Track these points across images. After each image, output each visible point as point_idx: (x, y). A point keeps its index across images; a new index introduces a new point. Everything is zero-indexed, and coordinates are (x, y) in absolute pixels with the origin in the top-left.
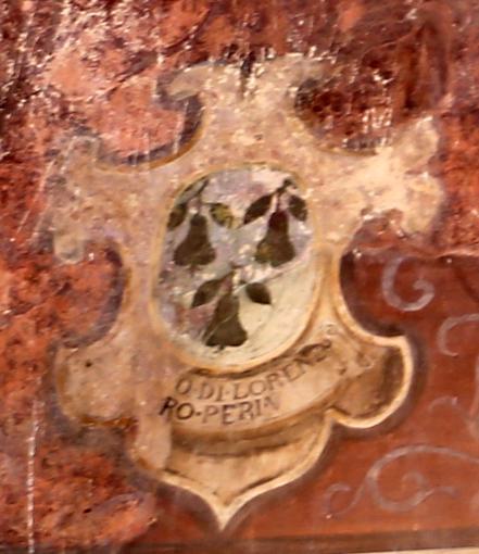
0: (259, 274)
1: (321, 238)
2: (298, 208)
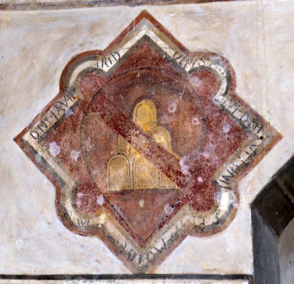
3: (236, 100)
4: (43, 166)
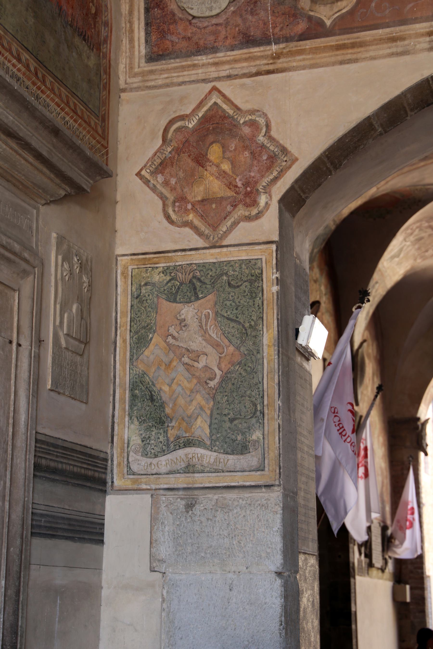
3: (271, 139)
4: (154, 189)
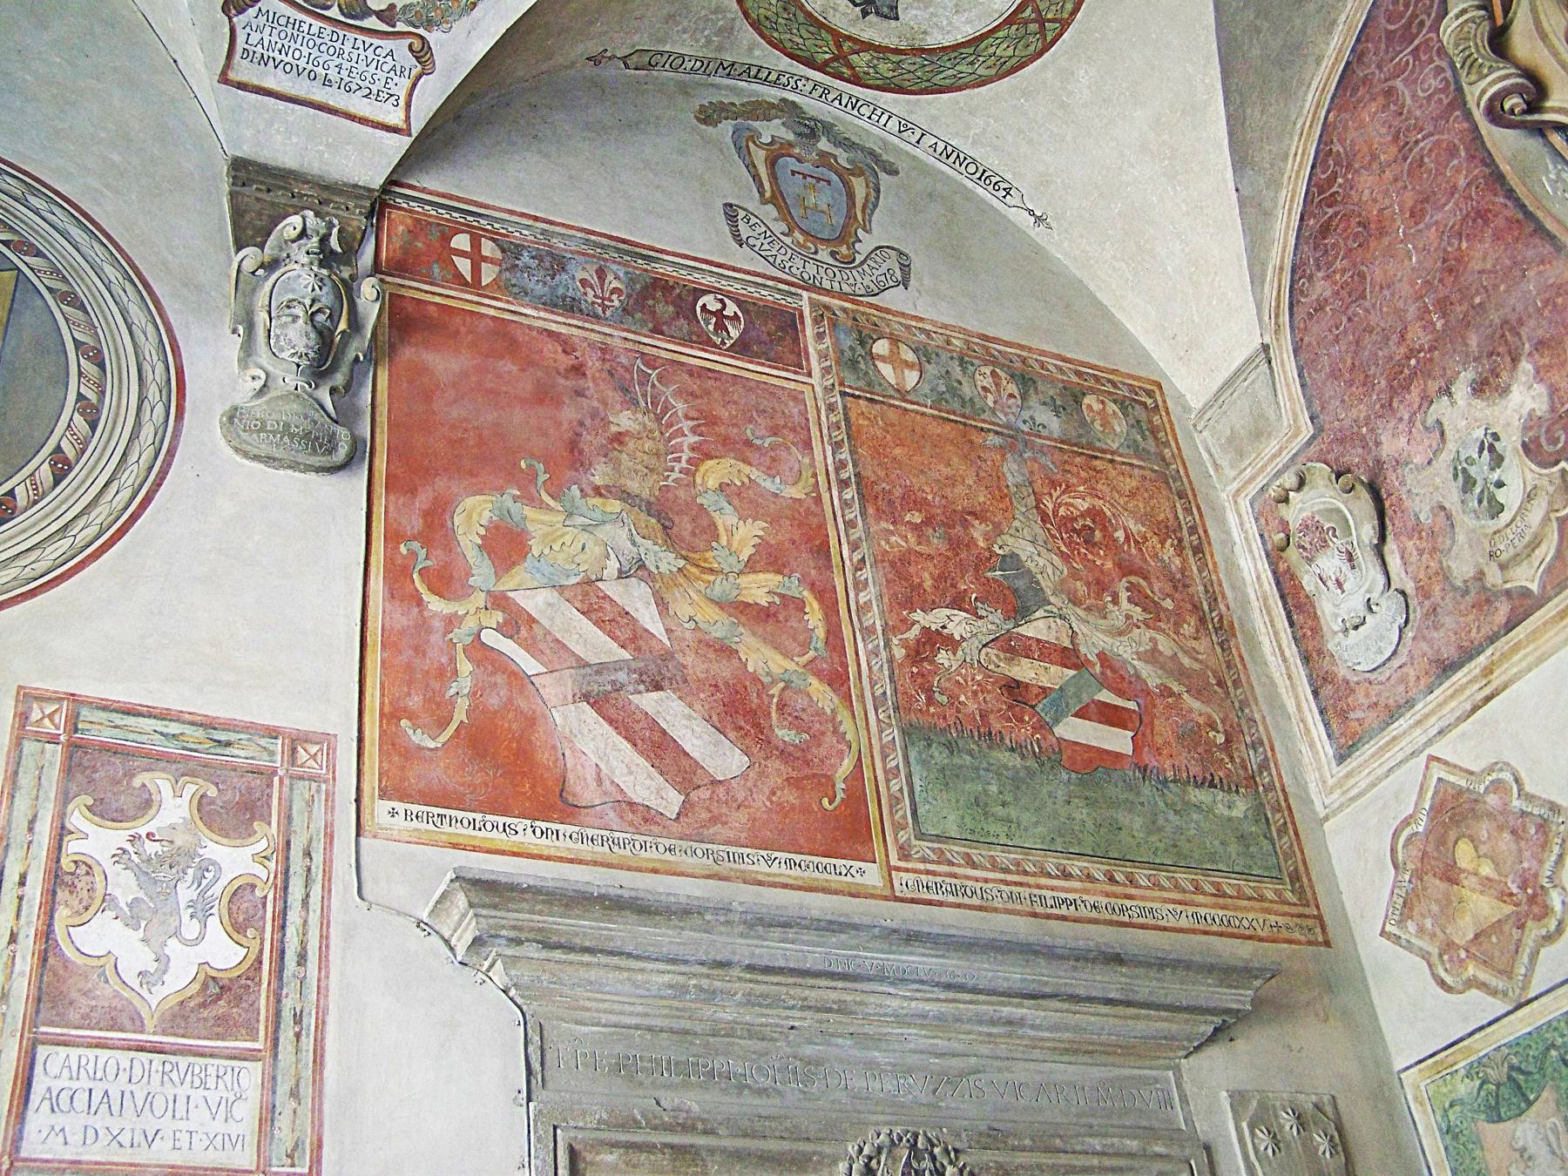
0: (1495, 476)
1: (1510, 443)
2: (1496, 437)
3: (1530, 798)
4: (1409, 947)
